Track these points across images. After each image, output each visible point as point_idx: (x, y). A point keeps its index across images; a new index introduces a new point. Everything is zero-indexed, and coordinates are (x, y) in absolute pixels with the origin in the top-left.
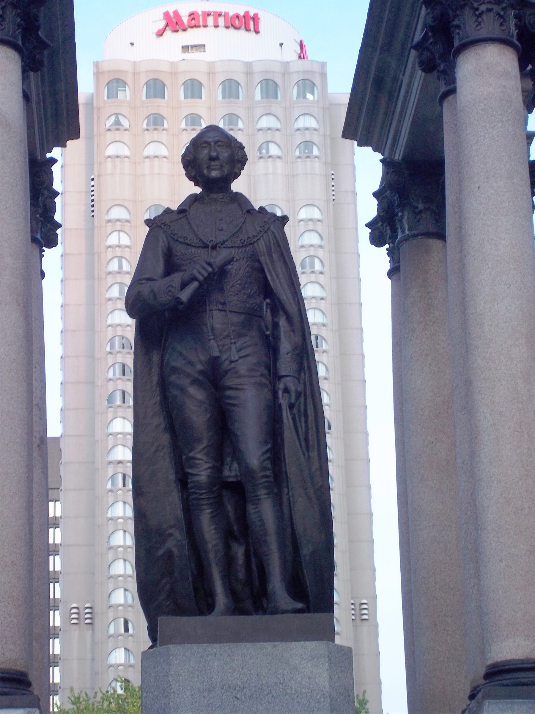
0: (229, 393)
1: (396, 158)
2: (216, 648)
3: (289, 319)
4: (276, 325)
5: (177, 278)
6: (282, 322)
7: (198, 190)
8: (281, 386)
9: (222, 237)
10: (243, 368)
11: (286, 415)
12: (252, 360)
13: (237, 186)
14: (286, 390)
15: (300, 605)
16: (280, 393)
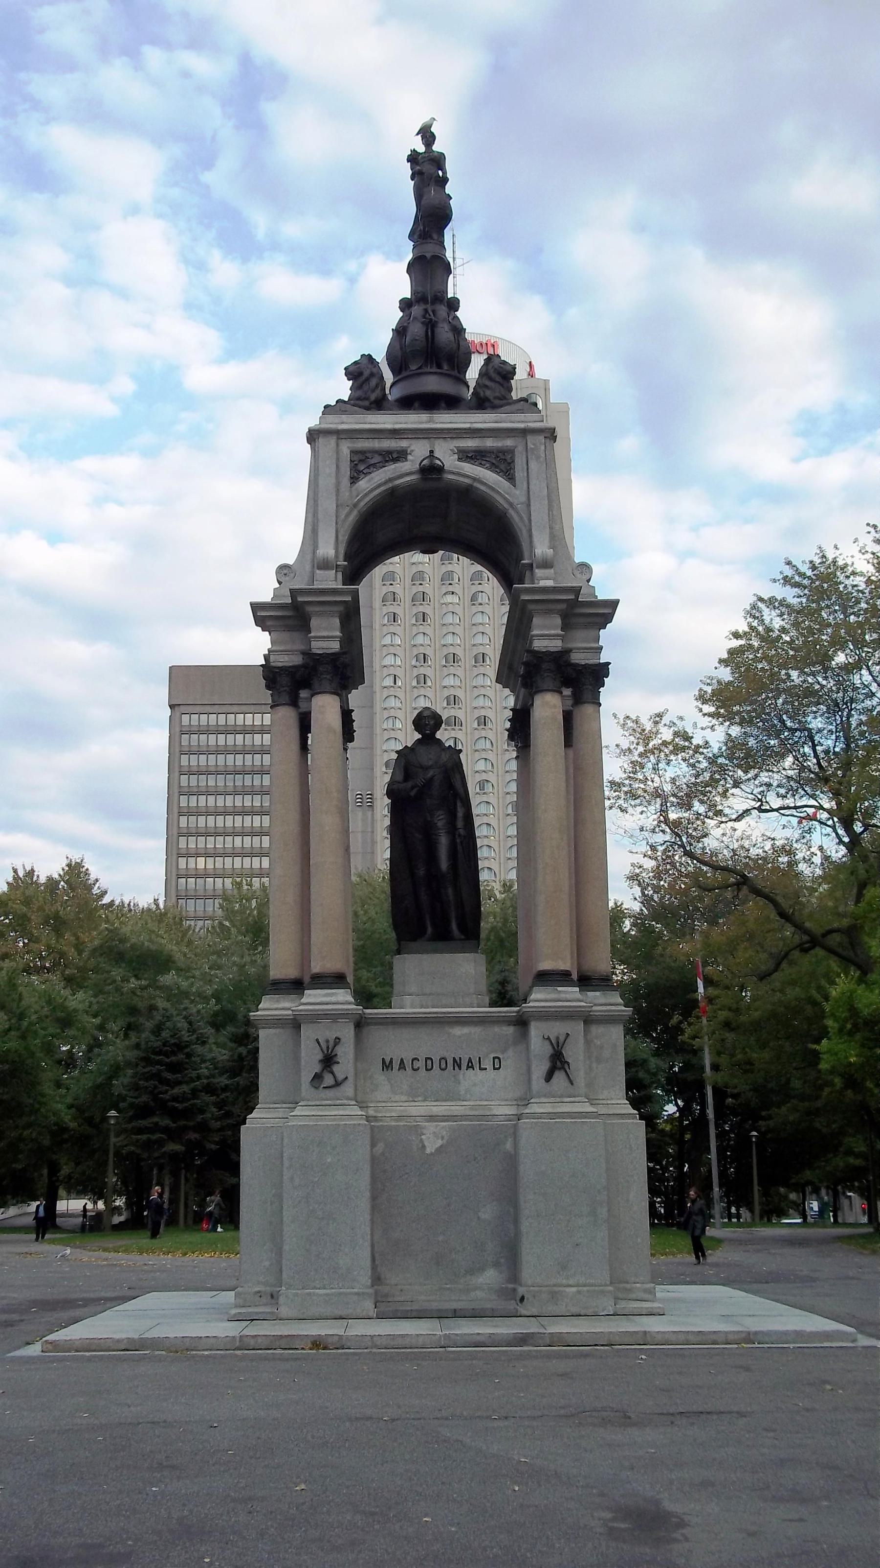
0: (434, 837)
1: (518, 708)
2: (425, 956)
3: (462, 802)
4: (455, 804)
5: (409, 784)
6: (459, 804)
7: (420, 736)
8: (457, 833)
9: (430, 763)
10: (440, 824)
11: (459, 847)
12: (444, 821)
13: (438, 735)
14: (460, 835)
15: (463, 937)
16: (457, 836)
